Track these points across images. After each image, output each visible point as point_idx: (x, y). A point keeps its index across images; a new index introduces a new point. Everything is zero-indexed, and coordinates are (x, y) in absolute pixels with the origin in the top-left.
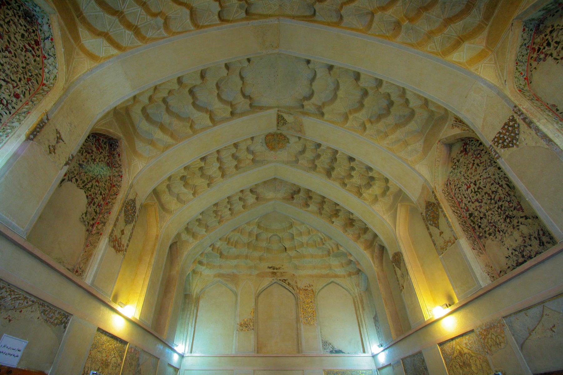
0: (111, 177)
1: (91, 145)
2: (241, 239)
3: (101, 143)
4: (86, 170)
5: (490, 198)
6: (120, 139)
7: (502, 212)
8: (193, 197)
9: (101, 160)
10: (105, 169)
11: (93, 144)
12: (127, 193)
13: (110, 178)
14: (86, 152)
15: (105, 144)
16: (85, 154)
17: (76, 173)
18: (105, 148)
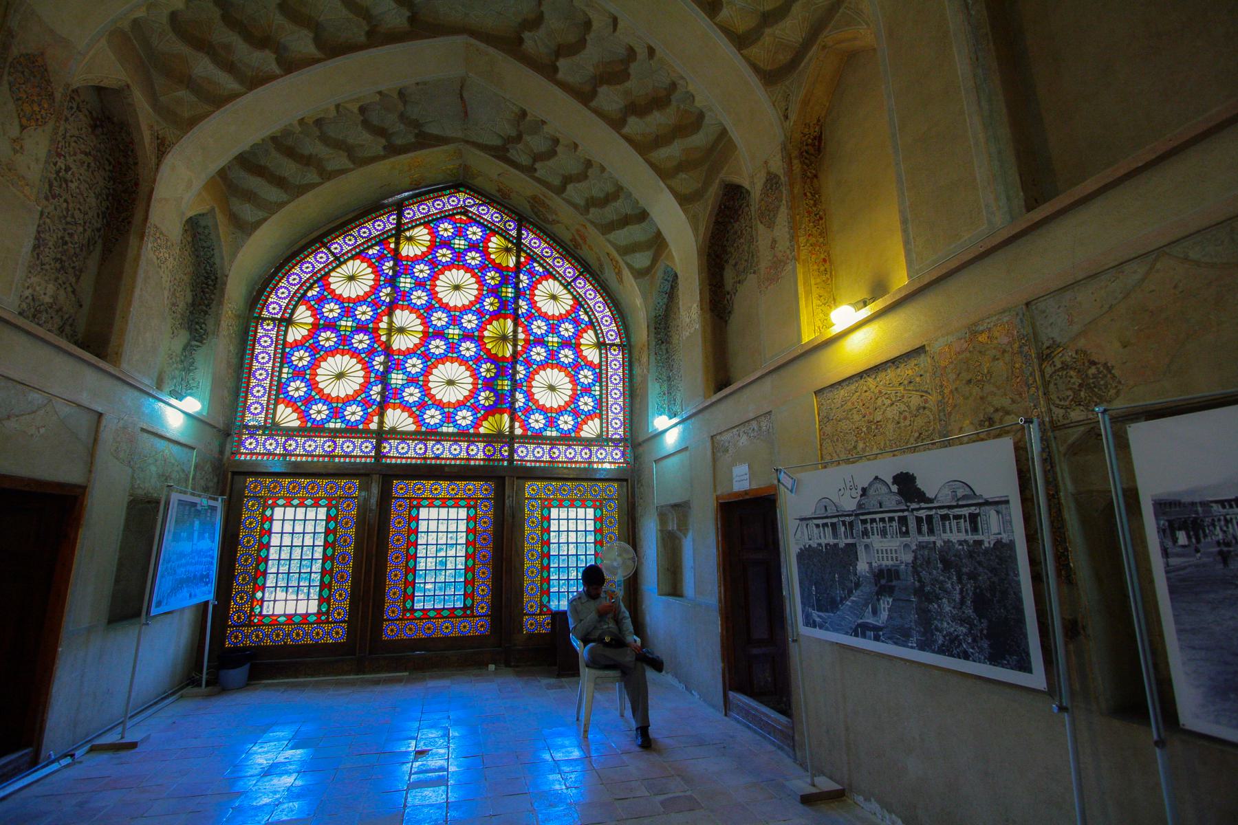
5: (65, 213)
7: (60, 249)
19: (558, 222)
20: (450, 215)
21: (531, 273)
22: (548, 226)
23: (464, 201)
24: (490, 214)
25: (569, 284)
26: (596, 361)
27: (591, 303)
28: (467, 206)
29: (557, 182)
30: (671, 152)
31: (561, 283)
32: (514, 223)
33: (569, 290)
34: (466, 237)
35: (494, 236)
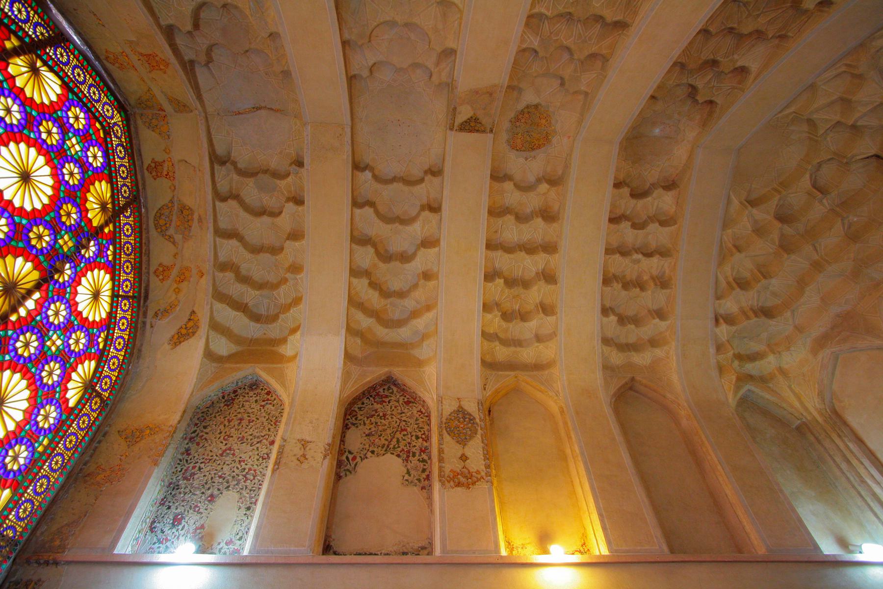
0: (422, 410)
1: (371, 406)
2: (755, 256)
3: (383, 393)
4: (379, 432)
6: (390, 372)
8: (554, 317)
9: (393, 408)
10: (406, 411)
11: (372, 404)
12: (438, 411)
13: (422, 412)
14: (368, 418)
15: (389, 388)
16: (367, 422)
17: (367, 446)
18: (392, 393)
19: (174, 243)
20: (93, 114)
21: (101, 252)
22: (153, 233)
23: (115, 124)
24: (120, 160)
25: (118, 296)
26: (72, 404)
27: (117, 333)
28: (113, 131)
29: (223, 224)
30: (365, 322)
31: (113, 289)
32: (129, 194)
33: (112, 301)
34: (85, 150)
35: (107, 183)
